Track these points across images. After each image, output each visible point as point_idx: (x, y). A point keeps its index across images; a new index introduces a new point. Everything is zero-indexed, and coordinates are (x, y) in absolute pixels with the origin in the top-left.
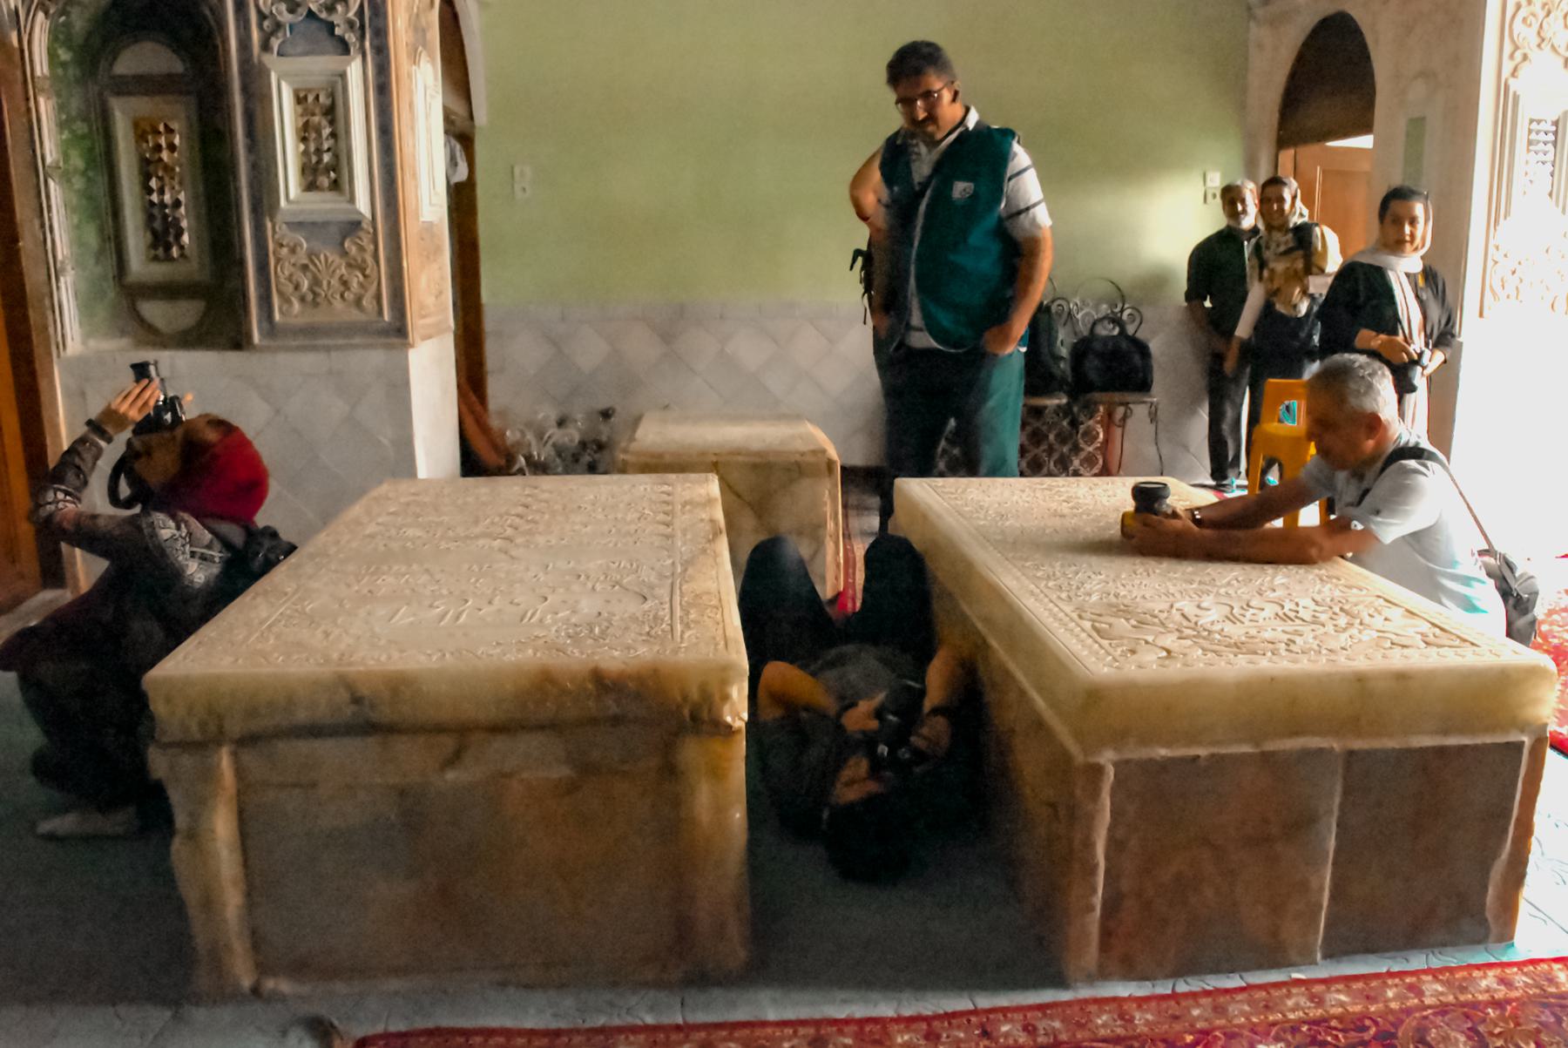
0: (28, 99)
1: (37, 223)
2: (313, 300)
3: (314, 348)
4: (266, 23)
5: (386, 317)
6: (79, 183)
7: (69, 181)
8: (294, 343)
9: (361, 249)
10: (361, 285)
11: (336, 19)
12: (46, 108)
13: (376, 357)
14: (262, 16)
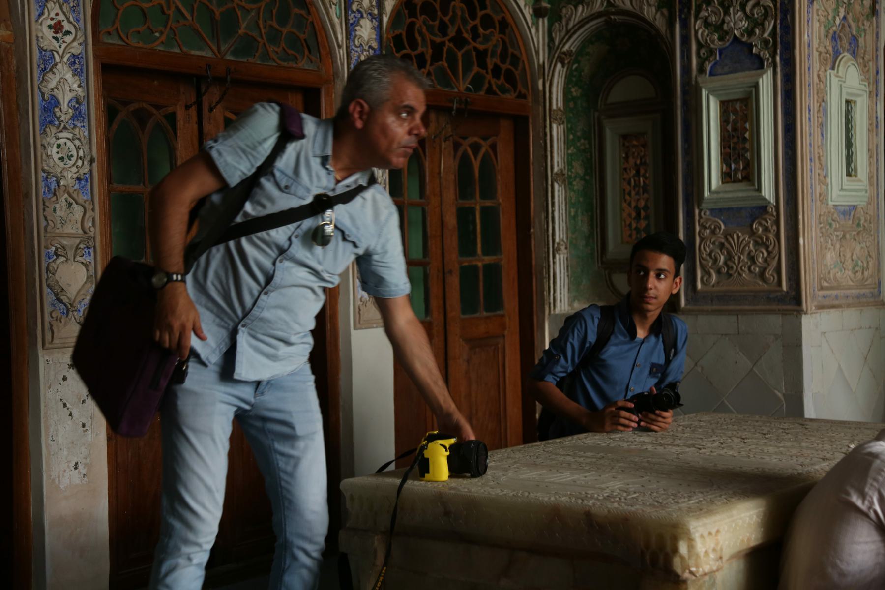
0: (545, 127)
1: (543, 215)
2: (727, 273)
3: (729, 312)
4: (703, 51)
5: (784, 287)
6: (578, 185)
7: (570, 183)
8: (709, 308)
9: (766, 229)
10: (765, 260)
11: (755, 41)
12: (557, 131)
13: (774, 321)
14: (700, 45)
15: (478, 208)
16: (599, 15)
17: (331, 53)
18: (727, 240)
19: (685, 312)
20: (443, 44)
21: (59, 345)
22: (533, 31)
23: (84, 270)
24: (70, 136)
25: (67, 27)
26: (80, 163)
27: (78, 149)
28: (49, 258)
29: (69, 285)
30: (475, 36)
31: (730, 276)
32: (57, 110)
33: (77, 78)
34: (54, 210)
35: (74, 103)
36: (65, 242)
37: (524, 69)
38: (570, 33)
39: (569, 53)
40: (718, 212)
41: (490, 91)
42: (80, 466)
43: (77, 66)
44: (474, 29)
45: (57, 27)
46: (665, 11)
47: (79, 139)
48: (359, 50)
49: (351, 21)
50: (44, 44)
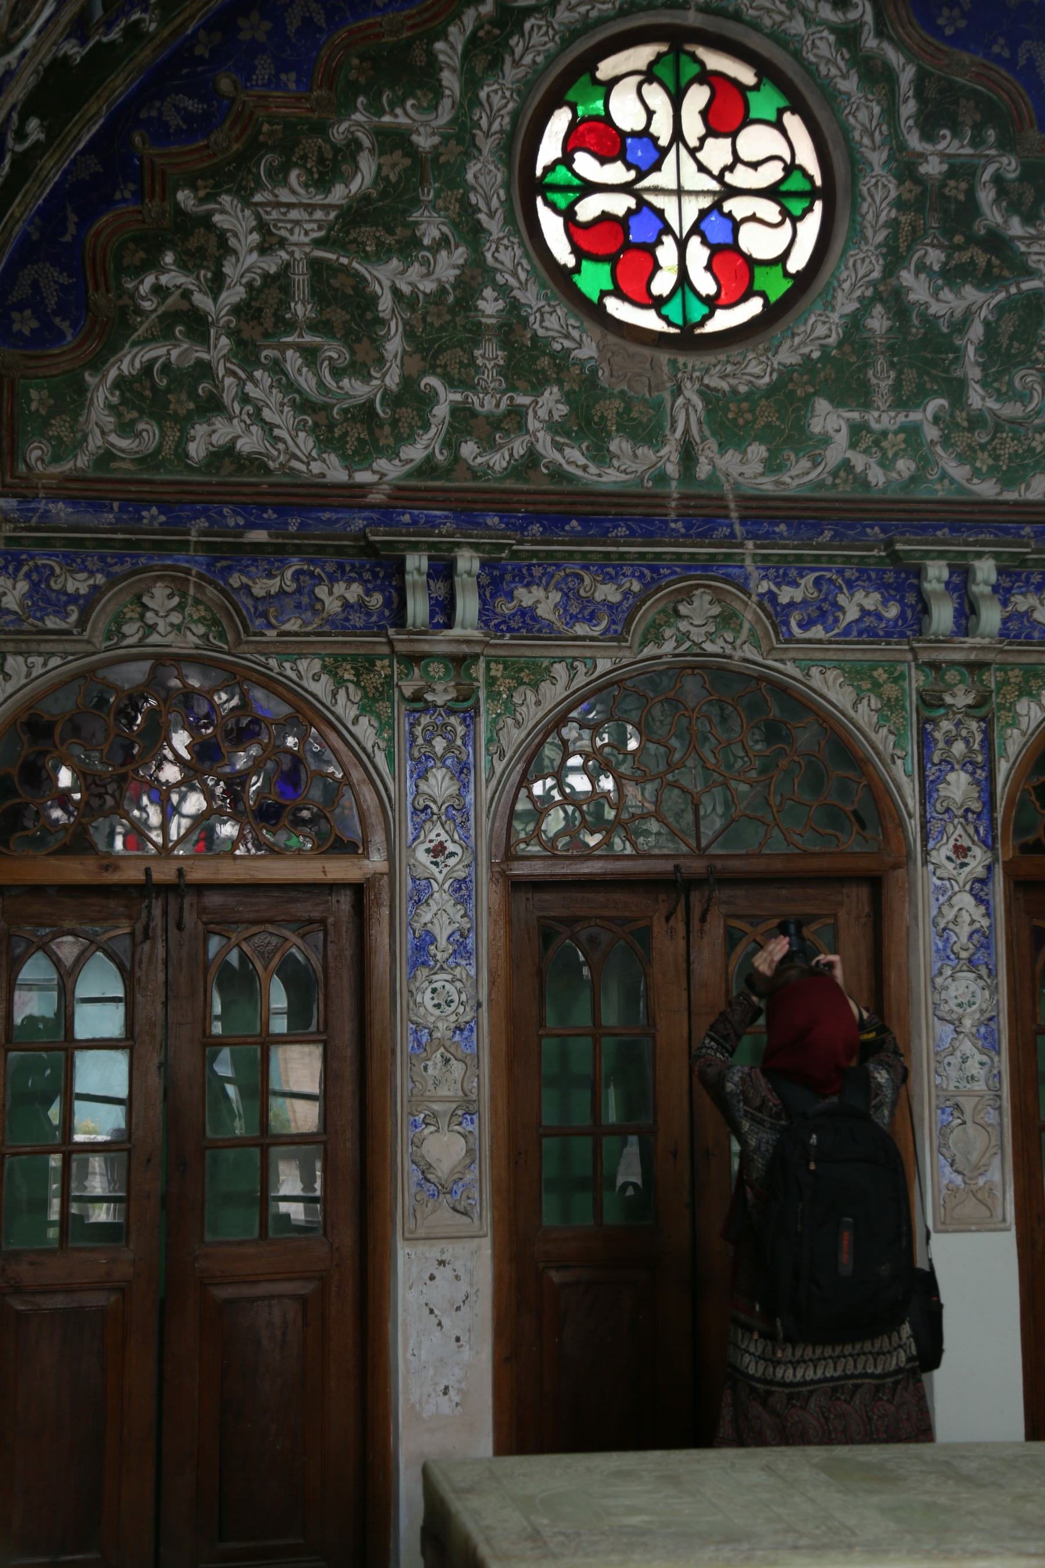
17: (901, 825)
23: (463, 1141)
24: (449, 977)
25: (451, 847)
26: (461, 1009)
27: (460, 992)
29: (440, 1160)
33: (459, 907)
34: (426, 1068)
35: (457, 936)
36: (436, 1107)
42: (452, 1392)
43: (463, 892)
45: (438, 850)
48: (946, 816)
49: (931, 778)
50: (419, 873)
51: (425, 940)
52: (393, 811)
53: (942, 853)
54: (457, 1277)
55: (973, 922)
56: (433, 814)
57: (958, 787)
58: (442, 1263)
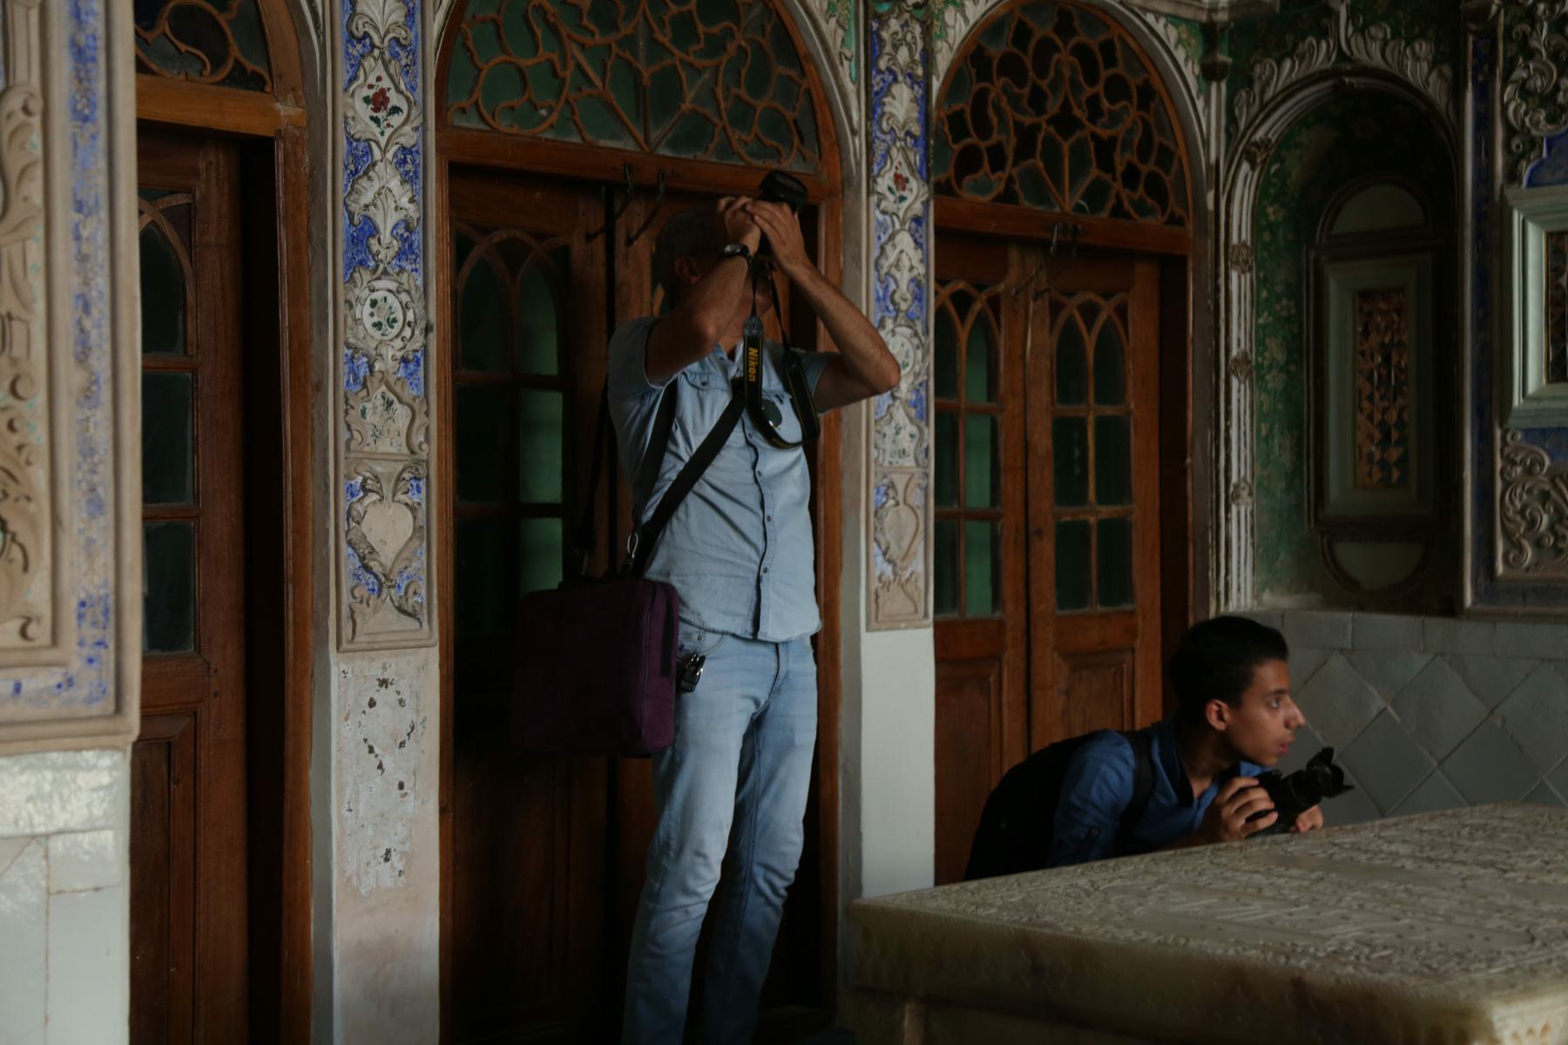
0: (1217, 276)
1: (1209, 435)
4: (1516, 142)
6: (1274, 381)
7: (1261, 378)
8: (1519, 609)
12: (1238, 284)
14: (1510, 131)
15: (1091, 419)
16: (1322, 76)
17: (839, 144)
18: (1555, 486)
19: (1472, 616)
20: (1036, 128)
21: (364, 646)
22: (1200, 104)
24: (393, 286)
25: (395, 99)
26: (407, 332)
27: (405, 308)
28: (352, 495)
29: (384, 542)
30: (1094, 111)
31: (1560, 552)
32: (373, 241)
33: (407, 187)
34: (363, 413)
35: (401, 230)
36: (379, 469)
37: (1181, 171)
38: (1267, 109)
39: (1265, 144)
40: (1538, 435)
41: (1118, 211)
42: (394, 857)
43: (409, 167)
44: (1093, 102)
45: (378, 101)
46: (1447, 70)
47: (408, 292)
48: (888, 138)
49: (876, 88)
50: (356, 130)
51: (366, 231)
52: (321, 33)
53: (885, 182)
54: (401, 702)
55: (912, 268)
56: (373, 46)
57: (901, 105)
58: (384, 683)
